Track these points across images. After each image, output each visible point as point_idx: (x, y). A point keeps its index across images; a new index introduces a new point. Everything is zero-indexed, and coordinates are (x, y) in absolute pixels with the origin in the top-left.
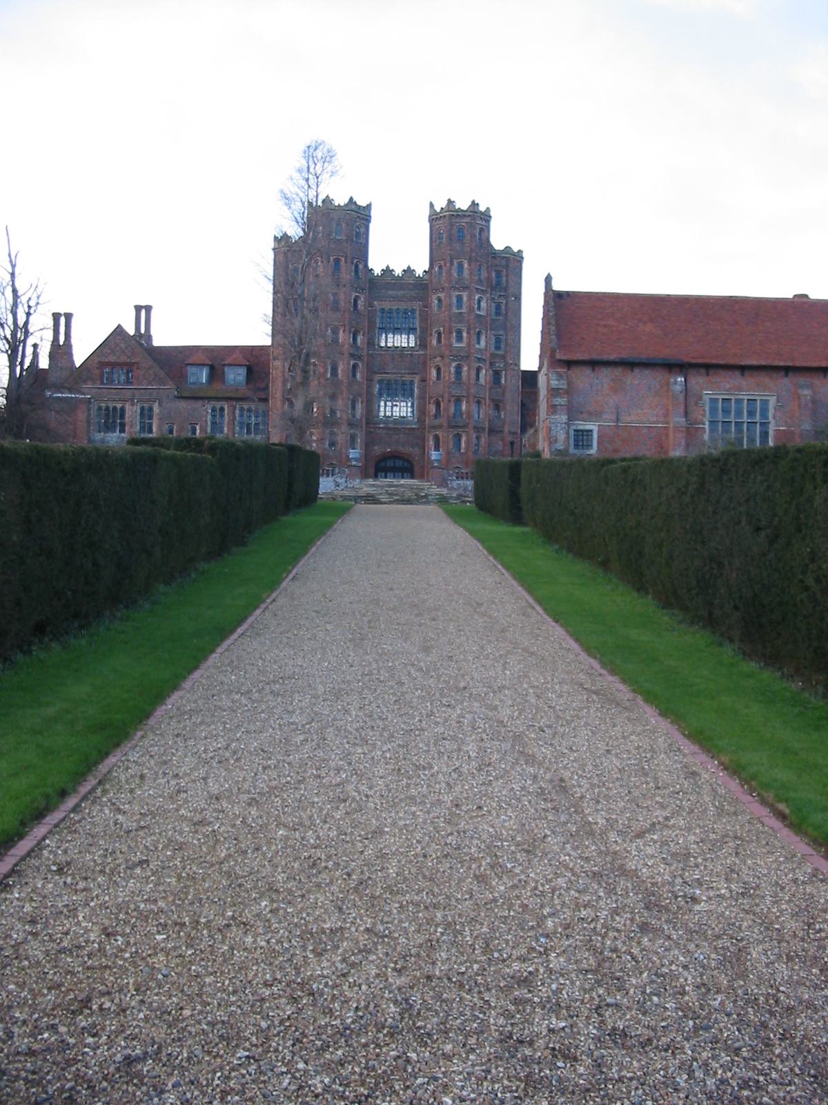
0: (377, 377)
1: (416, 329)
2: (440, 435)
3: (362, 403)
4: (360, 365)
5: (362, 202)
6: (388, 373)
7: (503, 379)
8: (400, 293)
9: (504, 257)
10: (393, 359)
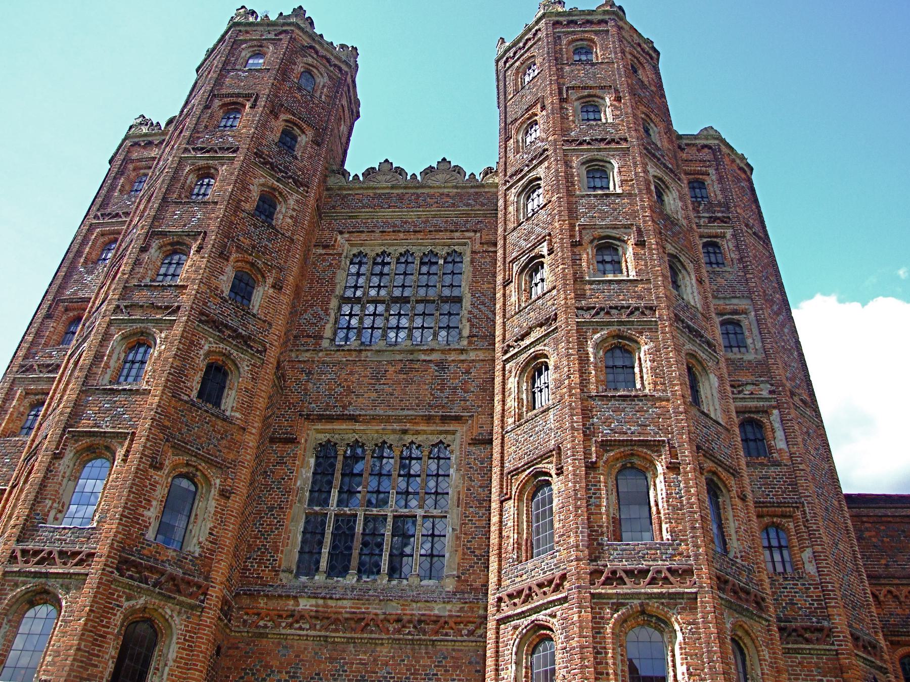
0: (313, 435)
1: (458, 300)
2: (555, 623)
3: (225, 494)
4: (245, 367)
5: (332, 29)
6: (353, 418)
7: (780, 434)
8: (413, 216)
9: (705, 146)
10: (378, 376)
